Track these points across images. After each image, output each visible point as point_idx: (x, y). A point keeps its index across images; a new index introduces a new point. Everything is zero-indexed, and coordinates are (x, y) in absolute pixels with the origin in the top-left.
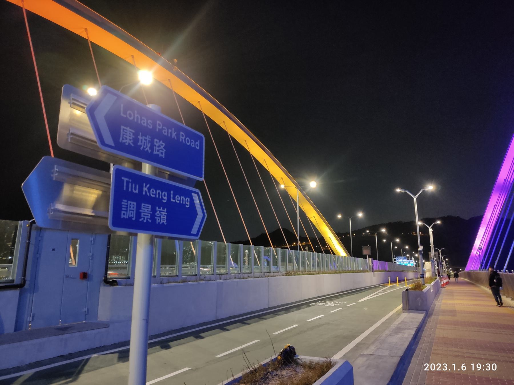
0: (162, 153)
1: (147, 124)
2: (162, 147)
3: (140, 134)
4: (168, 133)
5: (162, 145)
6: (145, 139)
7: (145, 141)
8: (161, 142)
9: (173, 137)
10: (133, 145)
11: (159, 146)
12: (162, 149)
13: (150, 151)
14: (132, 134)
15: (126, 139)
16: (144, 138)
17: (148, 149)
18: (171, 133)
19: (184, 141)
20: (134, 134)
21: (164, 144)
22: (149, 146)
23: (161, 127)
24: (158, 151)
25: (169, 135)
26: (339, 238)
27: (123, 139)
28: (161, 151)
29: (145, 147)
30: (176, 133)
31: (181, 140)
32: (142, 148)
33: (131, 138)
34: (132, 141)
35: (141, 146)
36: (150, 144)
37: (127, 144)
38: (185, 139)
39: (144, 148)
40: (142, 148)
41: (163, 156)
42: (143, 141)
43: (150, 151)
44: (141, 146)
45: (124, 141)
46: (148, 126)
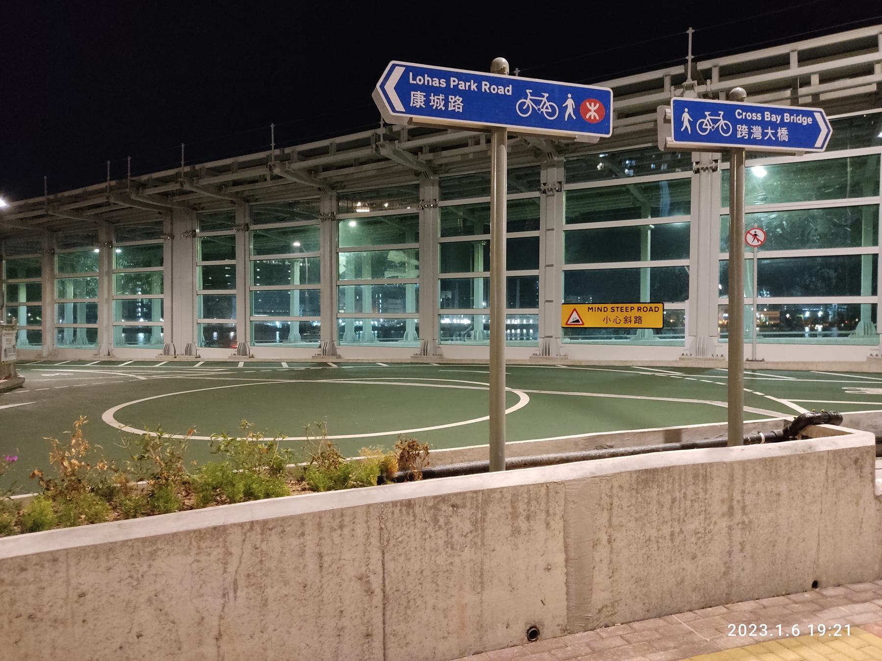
0: (459, 108)
1: (440, 83)
2: (459, 102)
3: (432, 94)
4: (465, 87)
5: (459, 100)
6: (438, 99)
7: (438, 101)
8: (457, 97)
9: (472, 89)
10: (424, 107)
11: (455, 102)
12: (458, 104)
13: (443, 108)
14: (423, 96)
15: (417, 102)
16: (436, 97)
17: (441, 106)
18: (470, 86)
19: (488, 91)
20: (424, 96)
21: (461, 99)
22: (442, 103)
23: (456, 83)
24: (454, 106)
25: (467, 89)
26: (628, 176)
27: (414, 103)
28: (457, 106)
29: (438, 105)
30: (476, 84)
31: (483, 91)
32: (434, 108)
33: (423, 101)
34: (423, 103)
35: (434, 105)
36: (444, 101)
37: (418, 107)
38: (489, 89)
39: (437, 107)
40: (434, 108)
41: (461, 110)
42: (436, 100)
43: (443, 108)
44: (434, 105)
45: (414, 105)
46: (441, 85)
